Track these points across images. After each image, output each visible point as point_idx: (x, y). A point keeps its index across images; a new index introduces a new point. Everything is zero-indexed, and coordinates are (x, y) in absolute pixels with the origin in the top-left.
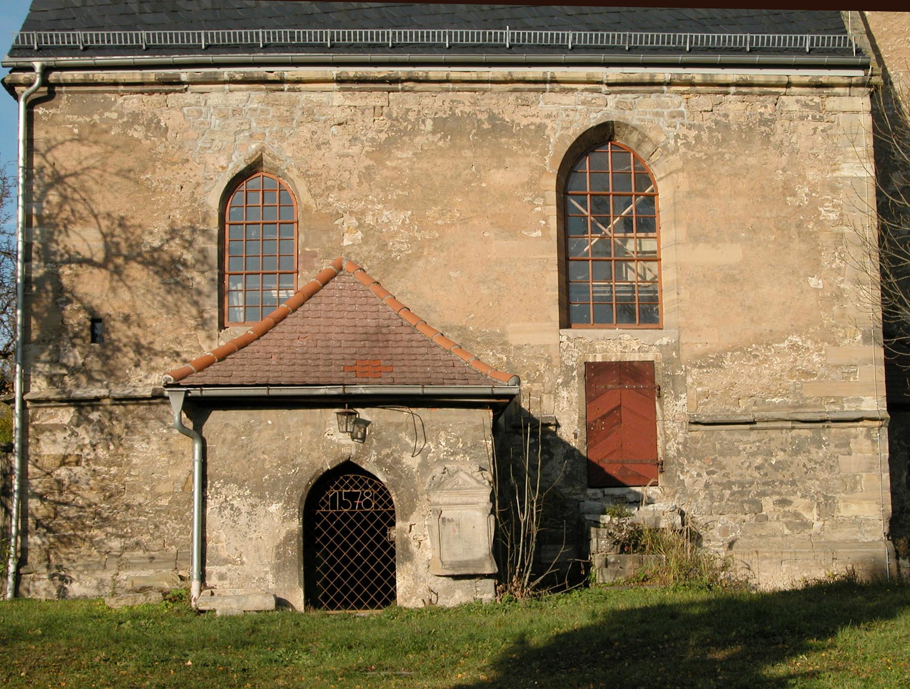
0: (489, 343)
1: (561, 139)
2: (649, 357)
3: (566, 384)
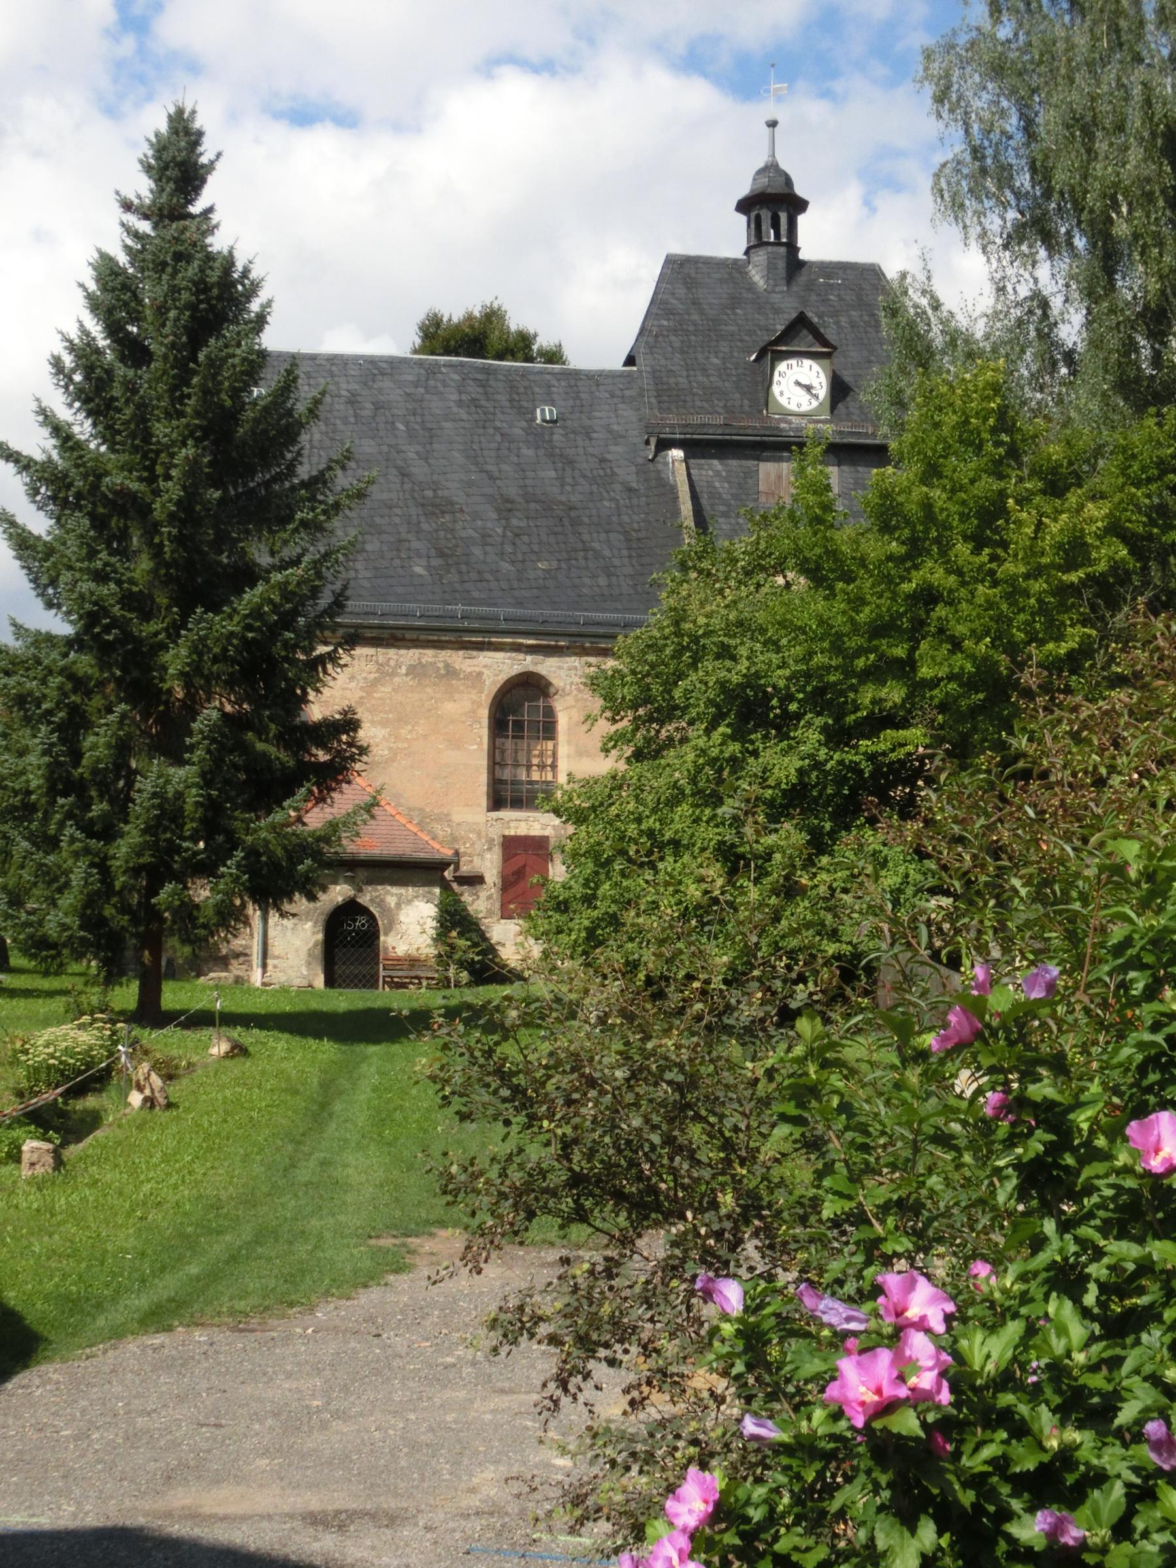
0: (438, 819)
1: (494, 682)
2: (546, 833)
3: (489, 849)
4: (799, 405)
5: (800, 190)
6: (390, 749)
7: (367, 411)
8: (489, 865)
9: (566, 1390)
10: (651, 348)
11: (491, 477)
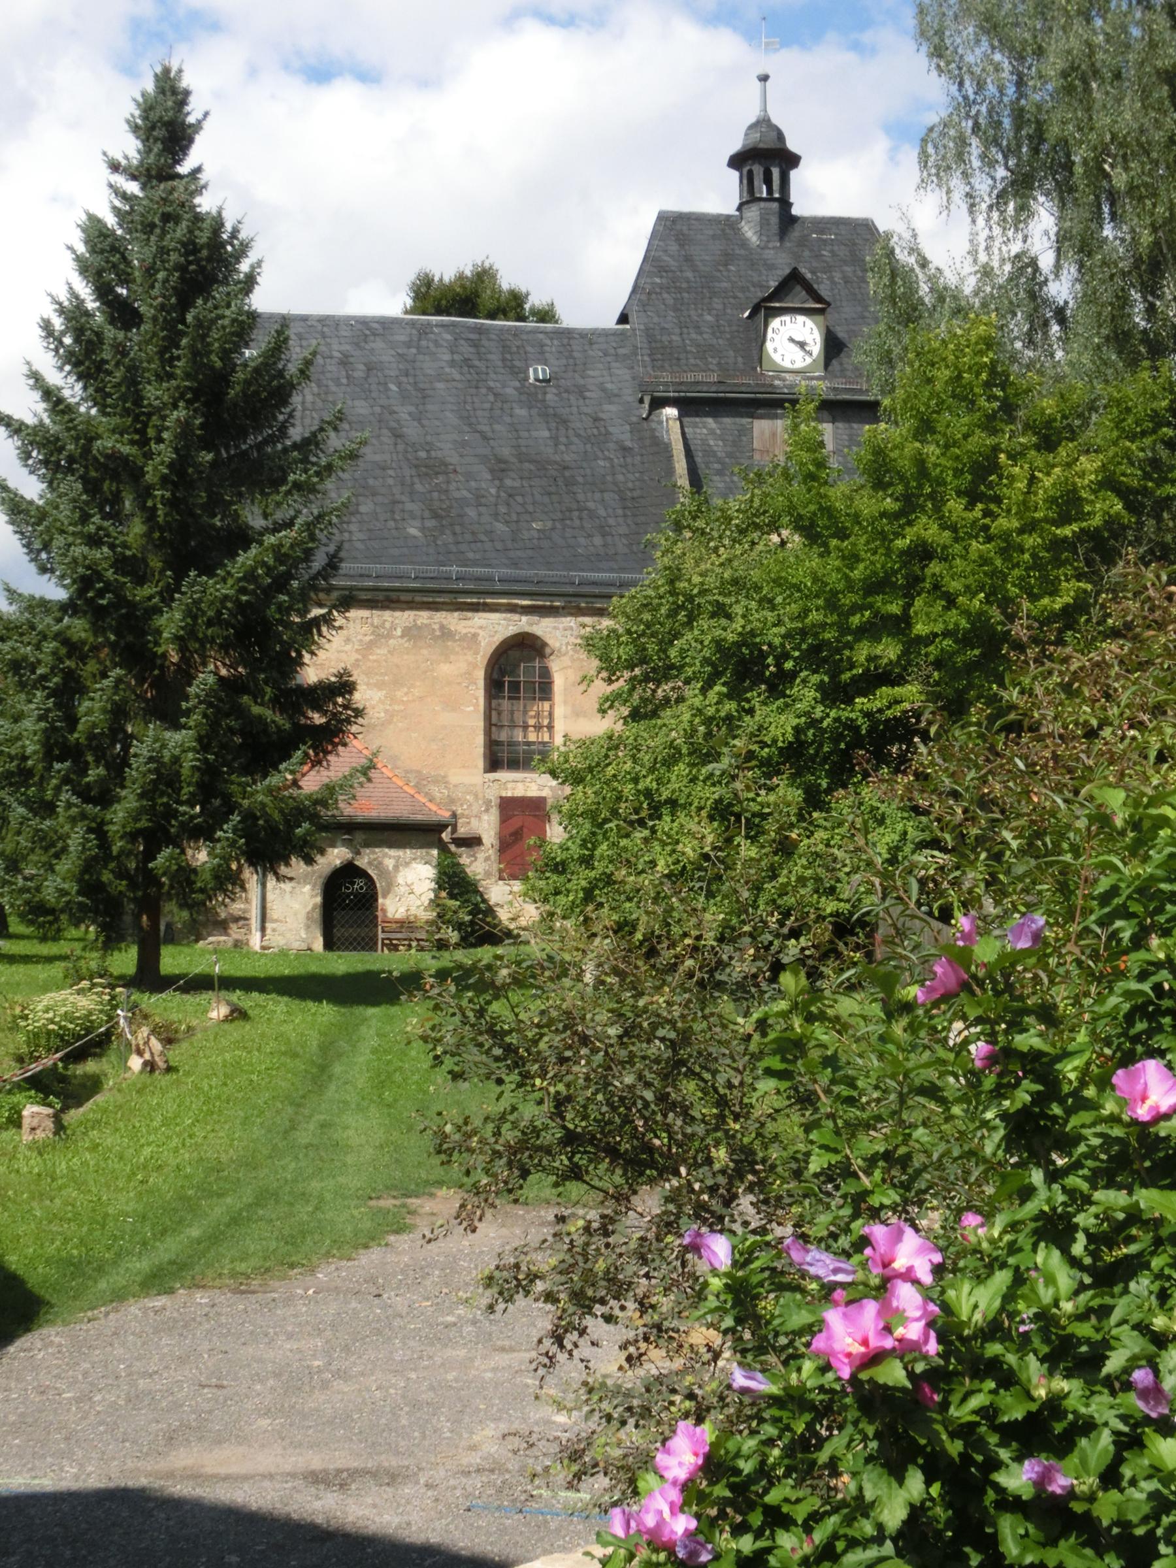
2: (543, 794)
3: (487, 810)
4: (793, 362)
5: (792, 145)
6: (386, 711)
7: (359, 372)
8: (487, 827)
9: (562, 1346)
10: (644, 306)
11: (485, 438)
